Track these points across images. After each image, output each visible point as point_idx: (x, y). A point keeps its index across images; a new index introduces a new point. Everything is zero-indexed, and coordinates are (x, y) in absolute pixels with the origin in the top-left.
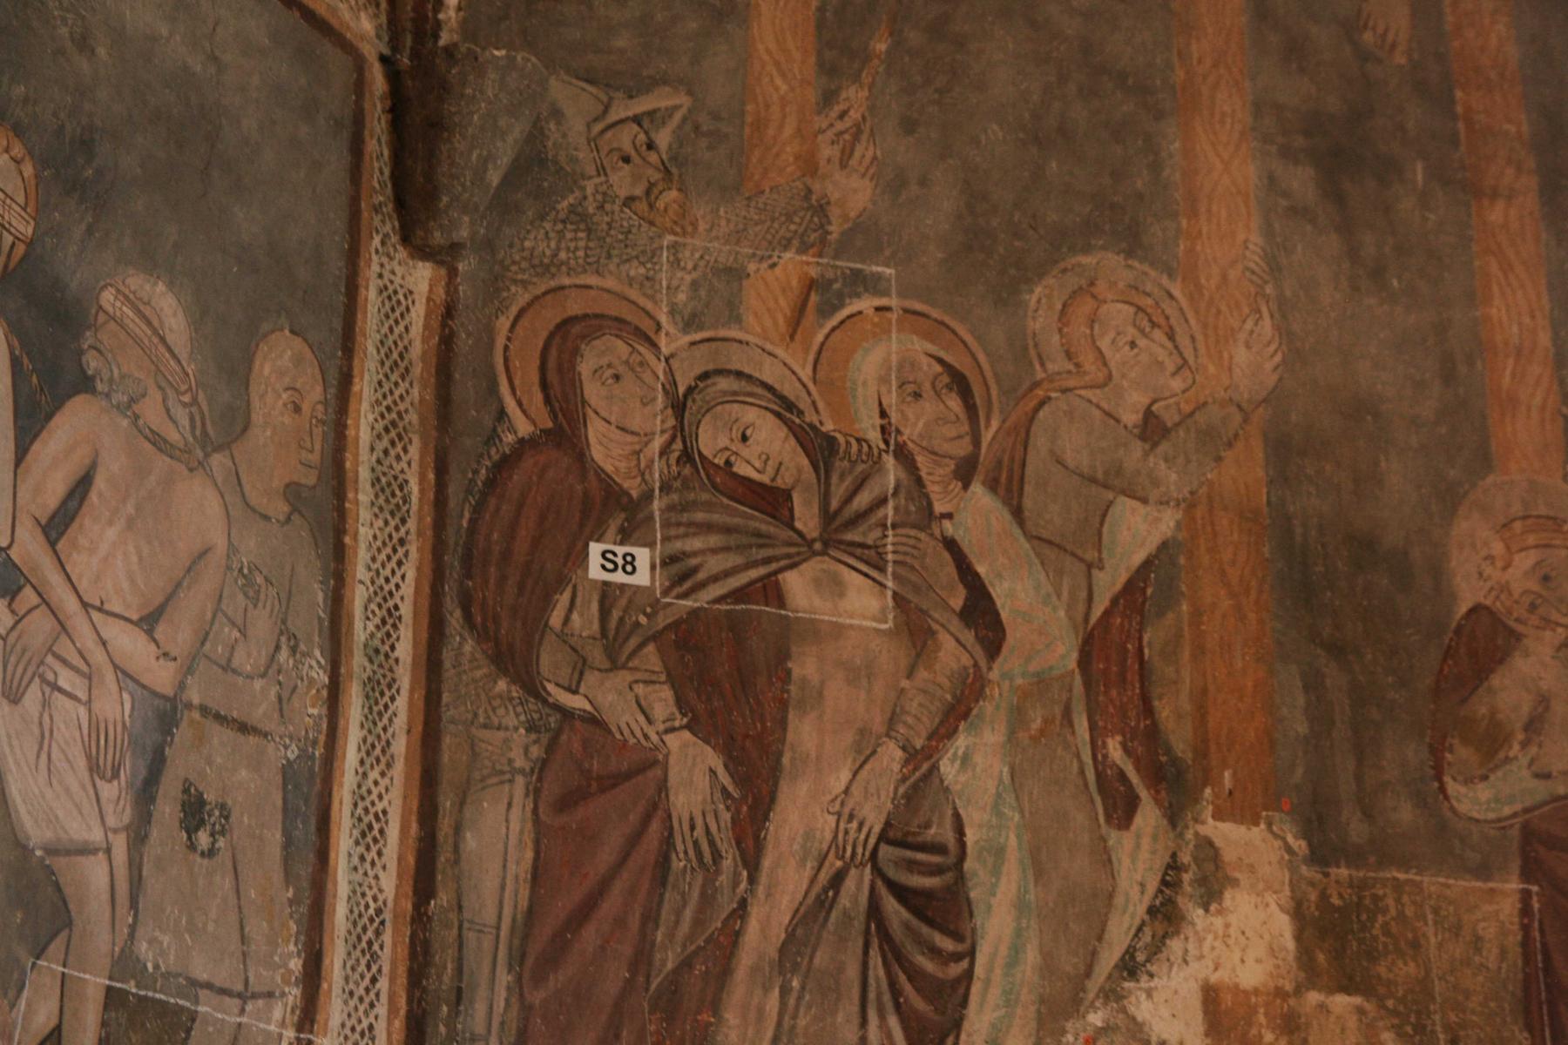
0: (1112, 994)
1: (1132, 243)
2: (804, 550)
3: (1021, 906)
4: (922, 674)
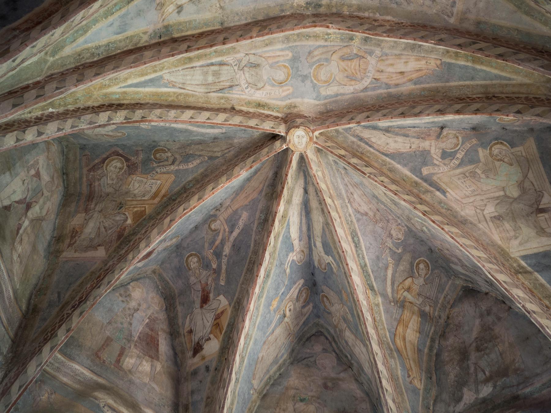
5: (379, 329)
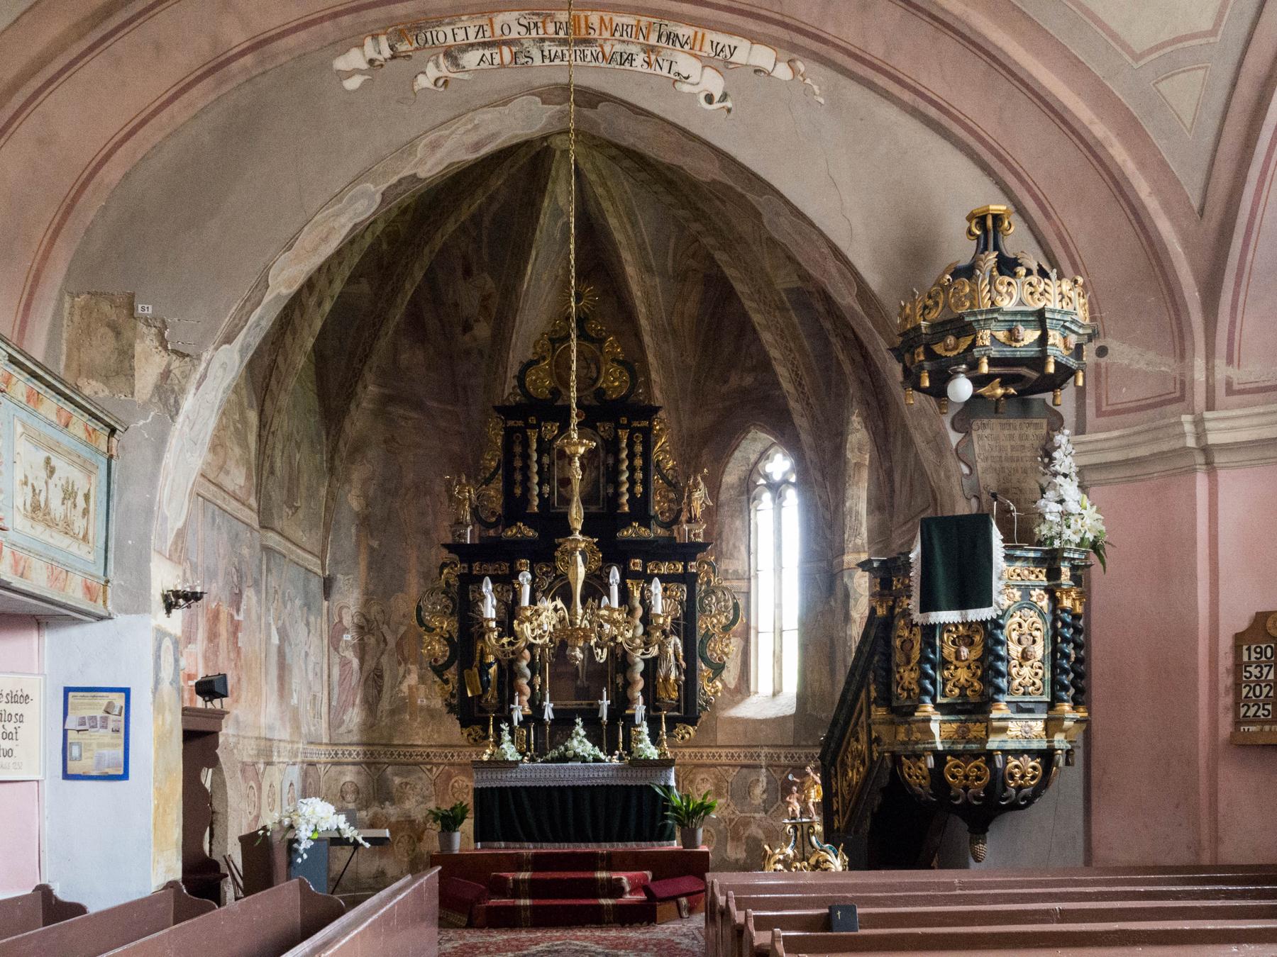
1: (402, 591)
2: (366, 634)
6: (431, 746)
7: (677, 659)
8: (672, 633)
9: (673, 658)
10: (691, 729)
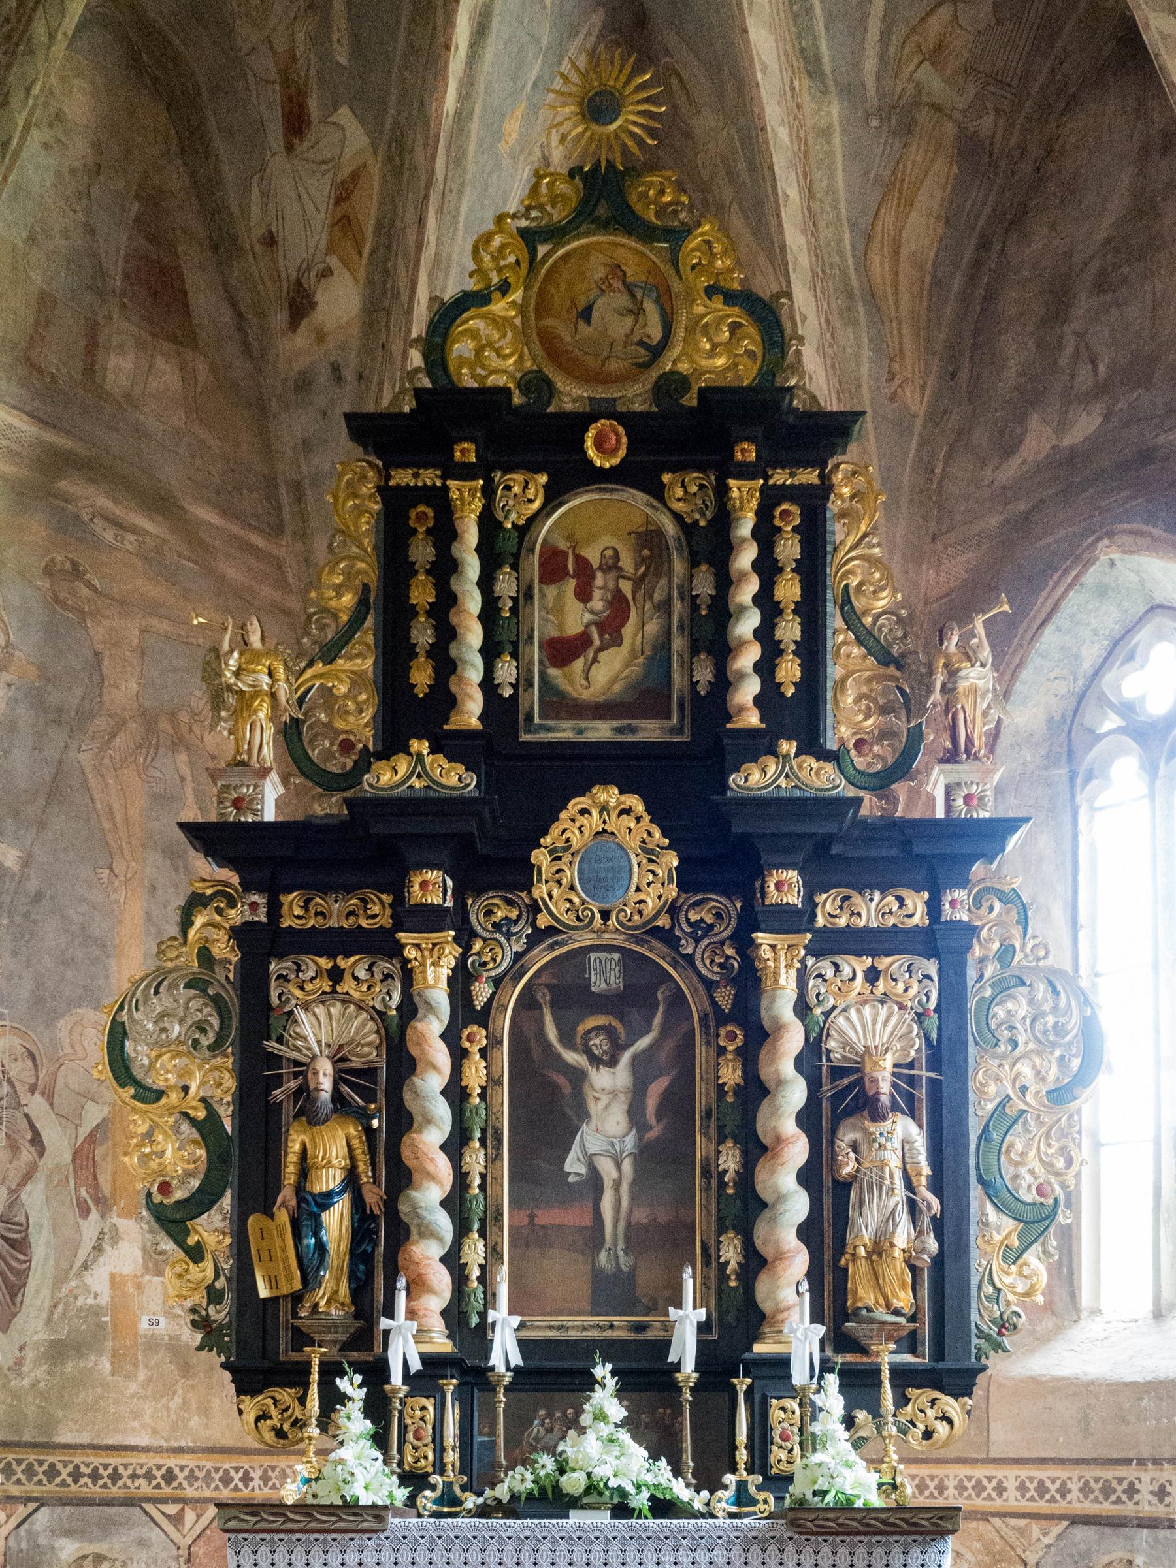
0: (79, 1275)
3: (48, 1244)
4: (15, 1163)
5: (821, 225)
6: (180, 1450)
7: (909, 1186)
8: (895, 1107)
9: (899, 1182)
10: (950, 1405)
